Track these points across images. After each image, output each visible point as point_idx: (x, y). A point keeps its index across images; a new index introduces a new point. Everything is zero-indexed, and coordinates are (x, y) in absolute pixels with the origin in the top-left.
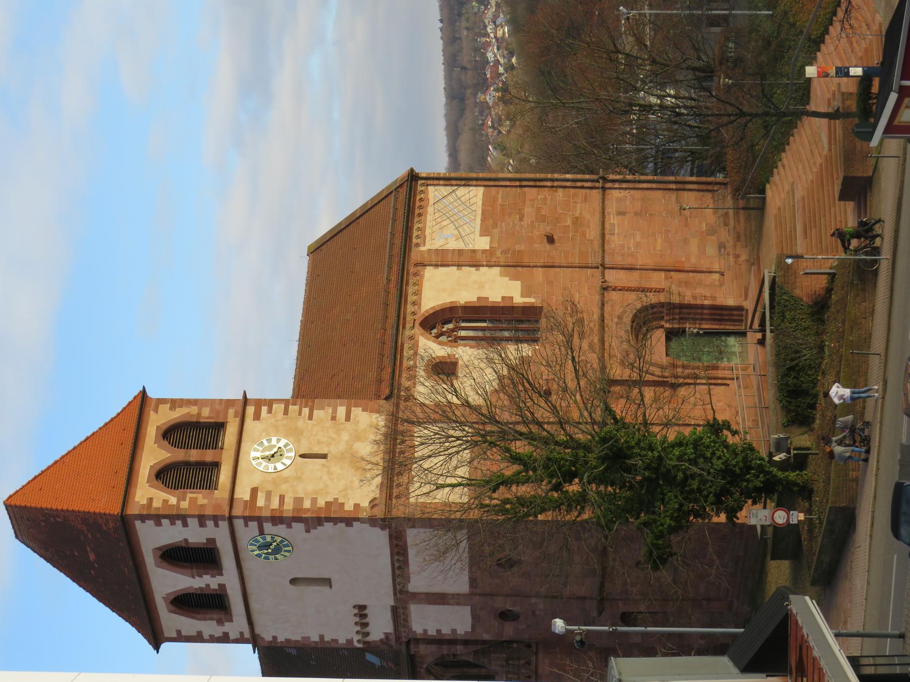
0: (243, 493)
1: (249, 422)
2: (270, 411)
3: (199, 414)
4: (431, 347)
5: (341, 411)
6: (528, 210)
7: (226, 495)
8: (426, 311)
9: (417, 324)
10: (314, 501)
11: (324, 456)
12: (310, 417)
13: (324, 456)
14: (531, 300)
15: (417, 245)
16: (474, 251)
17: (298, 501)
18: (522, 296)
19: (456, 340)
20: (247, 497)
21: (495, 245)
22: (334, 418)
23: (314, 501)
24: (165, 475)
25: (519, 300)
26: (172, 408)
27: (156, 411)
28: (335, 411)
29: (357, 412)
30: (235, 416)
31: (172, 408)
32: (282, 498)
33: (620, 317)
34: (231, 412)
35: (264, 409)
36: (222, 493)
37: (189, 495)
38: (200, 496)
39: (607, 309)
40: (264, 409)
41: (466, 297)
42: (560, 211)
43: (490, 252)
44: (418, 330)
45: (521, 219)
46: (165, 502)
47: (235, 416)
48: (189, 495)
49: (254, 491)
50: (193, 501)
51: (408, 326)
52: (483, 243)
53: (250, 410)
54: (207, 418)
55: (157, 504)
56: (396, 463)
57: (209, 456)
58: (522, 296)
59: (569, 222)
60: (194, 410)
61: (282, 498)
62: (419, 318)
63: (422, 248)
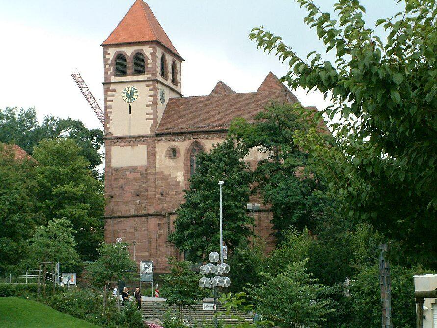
0: (113, 87)
1: (144, 84)
3: (148, 64)
7: (112, 81)
10: (111, 112)
11: (130, 113)
13: (130, 113)
17: (110, 107)
23: (111, 112)
24: (120, 57)
26: (150, 53)
28: (151, 114)
30: (148, 78)
32: (111, 101)
34: (150, 75)
35: (151, 88)
36: (113, 79)
38: (112, 71)
40: (151, 88)
44: (192, 141)
47: (148, 78)
50: (109, 69)
51: (194, 136)
53: (151, 83)
55: (108, 57)
56: (131, 140)
57: (129, 71)
60: (150, 61)
61: (111, 101)
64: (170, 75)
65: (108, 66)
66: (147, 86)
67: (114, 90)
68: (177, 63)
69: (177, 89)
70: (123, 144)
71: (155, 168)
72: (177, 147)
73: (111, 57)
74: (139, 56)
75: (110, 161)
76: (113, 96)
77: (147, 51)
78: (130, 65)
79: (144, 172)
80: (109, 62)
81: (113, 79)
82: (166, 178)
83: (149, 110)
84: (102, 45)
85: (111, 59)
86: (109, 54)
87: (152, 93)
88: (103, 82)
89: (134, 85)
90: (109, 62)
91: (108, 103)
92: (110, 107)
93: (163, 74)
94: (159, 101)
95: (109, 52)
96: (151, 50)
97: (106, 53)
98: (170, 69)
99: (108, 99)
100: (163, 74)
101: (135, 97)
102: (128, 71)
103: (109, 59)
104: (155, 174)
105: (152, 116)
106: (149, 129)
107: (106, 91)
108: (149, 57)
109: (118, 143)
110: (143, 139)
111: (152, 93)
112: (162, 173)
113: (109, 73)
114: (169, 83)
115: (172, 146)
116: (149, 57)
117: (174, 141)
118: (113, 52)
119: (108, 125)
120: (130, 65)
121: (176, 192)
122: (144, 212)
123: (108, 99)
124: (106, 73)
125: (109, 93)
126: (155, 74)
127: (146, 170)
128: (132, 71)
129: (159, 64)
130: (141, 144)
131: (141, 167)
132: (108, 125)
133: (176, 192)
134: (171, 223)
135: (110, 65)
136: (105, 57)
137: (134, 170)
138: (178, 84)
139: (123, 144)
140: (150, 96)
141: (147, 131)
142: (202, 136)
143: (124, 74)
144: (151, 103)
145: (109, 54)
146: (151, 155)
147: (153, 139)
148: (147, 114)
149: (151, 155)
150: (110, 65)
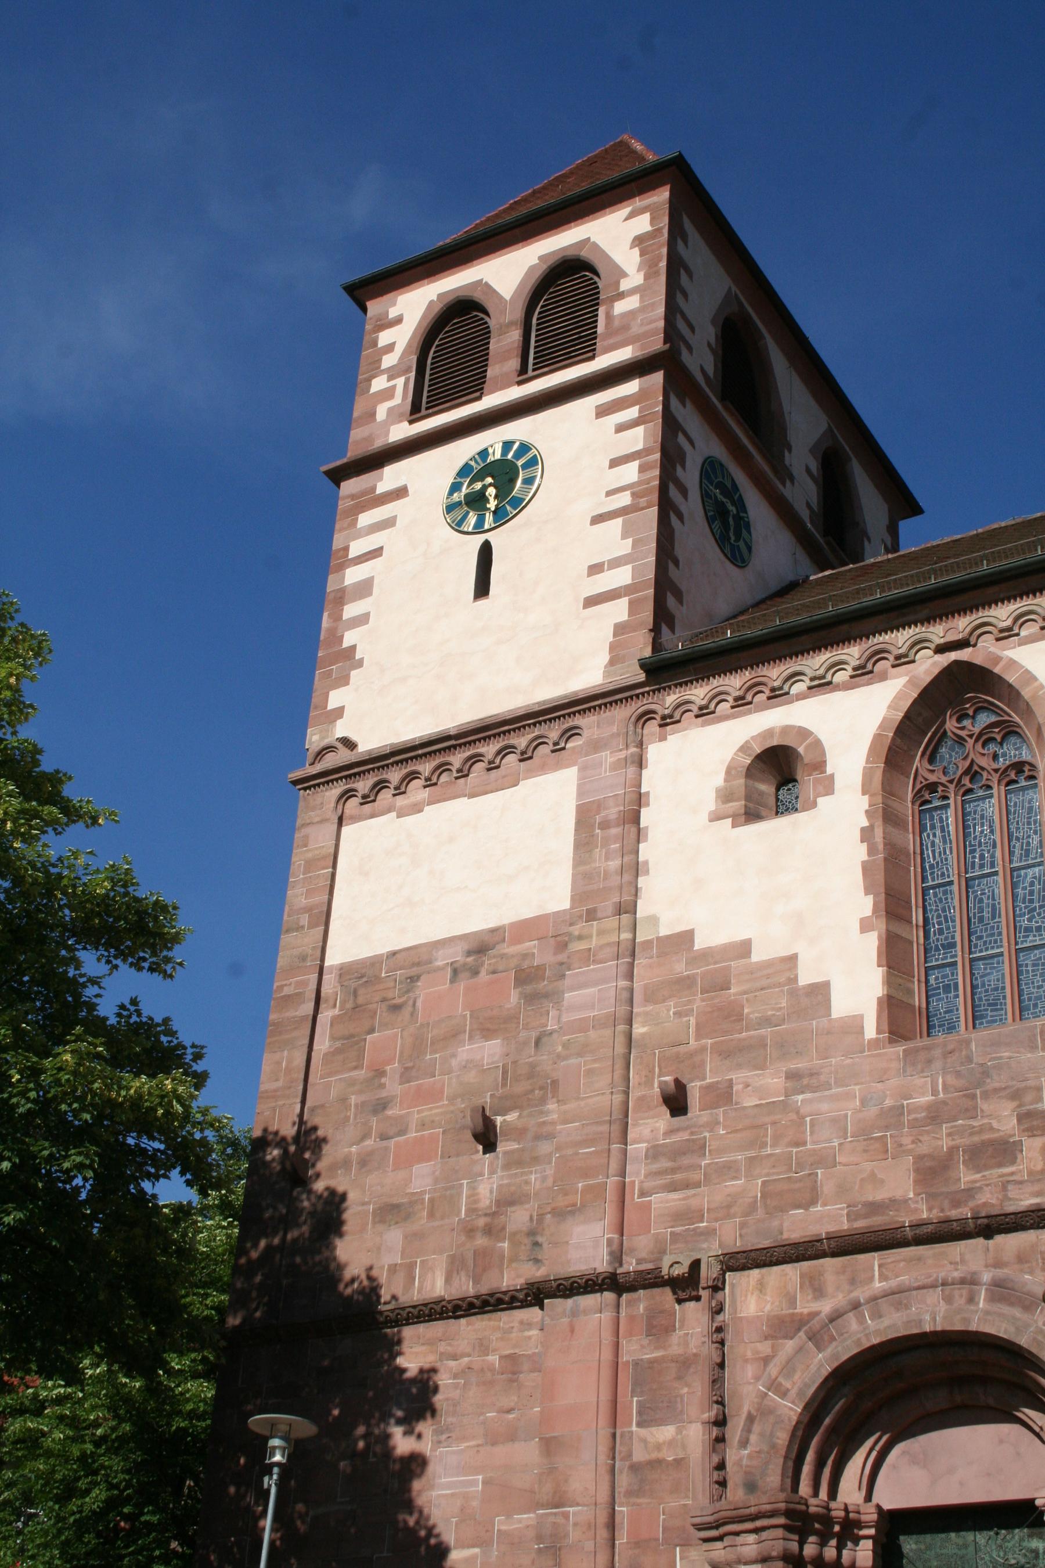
2: (621, 428)
4: (848, 716)
5: (623, 576)
8: (1012, 663)
9: (953, 656)
11: (482, 588)
12: (598, 519)
13: (482, 588)
20: (381, 488)
22: (595, 569)
28: (616, 563)
29: (619, 611)
33: (1003, 1291)
37: (400, 382)
44: (928, 665)
46: (390, 348)
48: (400, 382)
51: (938, 632)
54: (609, 316)
55: (384, 338)
62: (984, 652)
66: (602, 411)
67: (401, 493)
70: (417, 791)
72: (804, 733)
74: (571, 284)
76: (389, 523)
79: (543, 956)
81: (401, 431)
85: (399, 350)
92: (365, 588)
103: (390, 348)
109: (385, 795)
110: (553, 732)
112: (687, 937)
115: (769, 733)
117: (777, 695)
121: (792, 1076)
122: (511, 1278)
130: (543, 769)
133: (792, 1076)
134: (746, 1348)
135: (393, 373)
139: (425, 794)
140: (615, 463)
141: (590, 674)
142: (1002, 614)
144: (625, 499)
147: (623, 713)
148: (595, 569)
149: (614, 828)
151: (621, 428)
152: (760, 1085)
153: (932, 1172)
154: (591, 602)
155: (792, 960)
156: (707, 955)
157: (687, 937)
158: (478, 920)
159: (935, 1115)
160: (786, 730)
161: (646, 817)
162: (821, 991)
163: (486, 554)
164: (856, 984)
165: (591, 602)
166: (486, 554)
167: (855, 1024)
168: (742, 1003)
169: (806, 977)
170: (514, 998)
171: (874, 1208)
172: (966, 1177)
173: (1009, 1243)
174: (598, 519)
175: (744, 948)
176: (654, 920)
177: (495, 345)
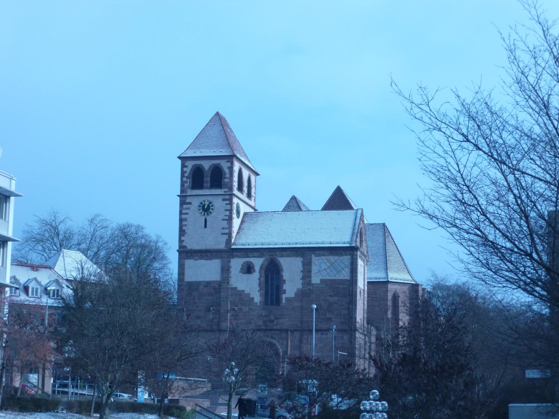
2: (227, 204)
3: (226, 178)
4: (258, 262)
6: (336, 299)
10: (186, 225)
11: (206, 226)
12: (223, 220)
13: (206, 226)
14: (284, 301)
15: (315, 254)
16: (310, 277)
17: (186, 220)
18: (286, 298)
19: (260, 272)
21: (315, 286)
22: (223, 228)
23: (186, 225)
25: (284, 296)
26: (229, 168)
27: (227, 162)
28: (226, 228)
31: (229, 168)
32: (187, 214)
34: (227, 190)
35: (228, 202)
36: (190, 192)
37: (188, 180)
38: (188, 184)
39: (277, 332)
41: (286, 275)
42: (335, 312)
43: (309, 283)
44: (268, 257)
45: (330, 296)
46: (186, 172)
48: (188, 180)
49: (190, 203)
50: (186, 182)
51: (269, 253)
52: (316, 280)
53: (227, 197)
55: (185, 169)
58: (286, 298)
59: (328, 316)
60: (228, 176)
61: (187, 214)
63: (313, 256)
64: (245, 189)
65: (185, 179)
66: (224, 200)
67: (190, 203)
68: (253, 178)
69: (252, 203)
71: (228, 283)
72: (252, 263)
73: (188, 170)
75: (183, 274)
76: (189, 209)
77: (225, 165)
78: (207, 179)
80: (186, 175)
82: (240, 294)
83: (225, 224)
84: (179, 157)
86: (187, 167)
87: (228, 207)
88: (179, 194)
89: (210, 199)
90: (186, 175)
91: (184, 216)
92: (186, 220)
93: (240, 189)
94: (235, 216)
95: (186, 164)
96: (229, 164)
97: (183, 166)
98: (245, 184)
99: (184, 211)
100: (240, 189)
101: (211, 210)
102: (205, 185)
103: (186, 172)
104: (228, 289)
105: (227, 231)
106: (224, 244)
107: (182, 203)
108: (227, 171)
111: (228, 207)
112: (236, 288)
113: (186, 185)
114: (244, 197)
116: (227, 171)
118: (190, 164)
119: (183, 238)
120: (207, 179)
121: (249, 309)
123: (184, 211)
124: (182, 185)
125: (185, 206)
126: (231, 189)
127: (220, 285)
128: (209, 185)
129: (236, 178)
131: (214, 282)
132: (183, 238)
133: (249, 309)
135: (187, 178)
136: (182, 170)
137: (208, 284)
138: (253, 199)
140: (226, 210)
143: (201, 187)
144: (227, 218)
145: (187, 167)
146: (225, 270)
148: (223, 228)
150: (187, 178)
151: (227, 204)
152: (245, 309)
153: (265, 322)
154: (223, 234)
155: (250, 294)
156: (239, 291)
157: (236, 288)
158: (207, 279)
159: (265, 316)
160: (250, 262)
161: (231, 270)
162: (253, 299)
163: (206, 220)
164: (257, 298)
165: (223, 234)
166: (206, 220)
167: (257, 303)
168: (242, 297)
169: (251, 297)
170: (213, 291)
171: (258, 326)
172: (268, 324)
173: (273, 332)
174: (223, 220)
175: (244, 291)
176: (232, 285)
177: (205, 179)
